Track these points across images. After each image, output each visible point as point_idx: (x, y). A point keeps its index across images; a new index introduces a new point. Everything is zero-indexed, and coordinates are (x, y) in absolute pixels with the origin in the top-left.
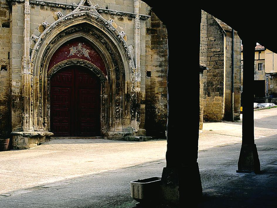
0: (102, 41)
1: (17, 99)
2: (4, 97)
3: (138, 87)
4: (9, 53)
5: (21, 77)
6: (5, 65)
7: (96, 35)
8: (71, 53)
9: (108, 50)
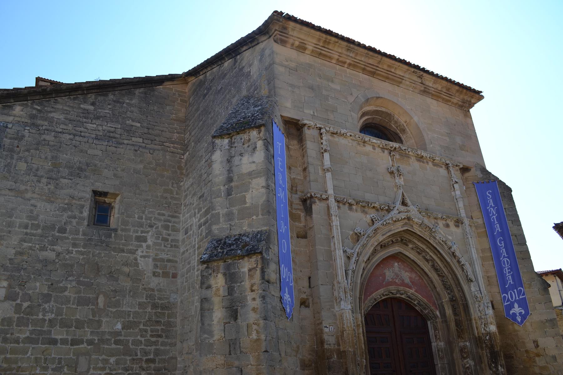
0: (428, 257)
1: (334, 355)
2: (310, 354)
3: (491, 324)
5: (335, 315)
6: (305, 297)
7: (418, 248)
8: (387, 278)
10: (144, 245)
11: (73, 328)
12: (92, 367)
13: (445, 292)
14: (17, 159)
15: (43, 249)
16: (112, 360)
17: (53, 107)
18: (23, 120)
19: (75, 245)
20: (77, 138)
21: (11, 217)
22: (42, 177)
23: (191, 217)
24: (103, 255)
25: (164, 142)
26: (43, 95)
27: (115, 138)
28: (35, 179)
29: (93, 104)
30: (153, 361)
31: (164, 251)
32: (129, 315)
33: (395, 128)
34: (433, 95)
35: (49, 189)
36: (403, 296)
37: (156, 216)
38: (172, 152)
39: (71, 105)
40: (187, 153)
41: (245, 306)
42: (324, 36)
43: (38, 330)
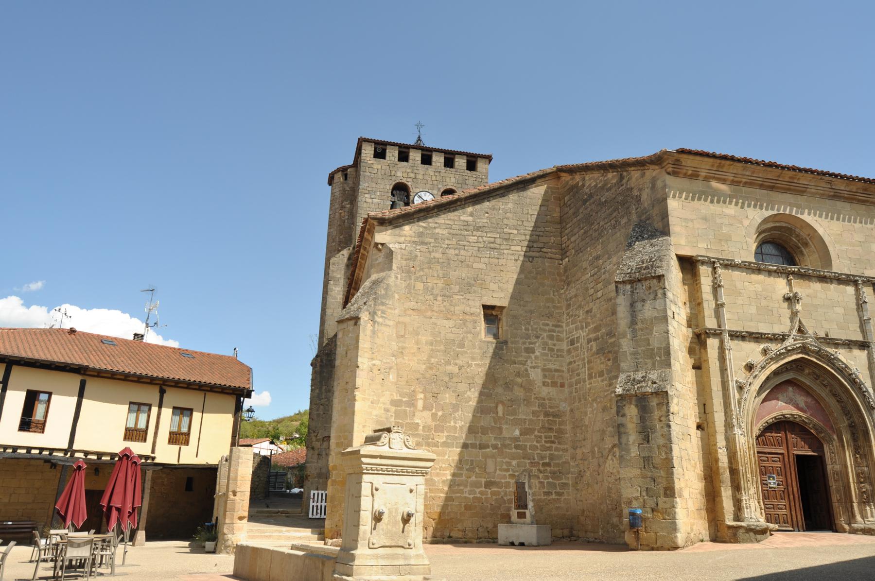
4: (704, 405)
9: (834, 395)
10: (533, 356)
11: (480, 434)
12: (498, 468)
13: (844, 417)
14: (415, 280)
15: (448, 363)
16: (514, 463)
17: (436, 223)
18: (413, 239)
19: (473, 359)
20: (463, 252)
21: (418, 334)
22: (437, 295)
23: (577, 329)
24: (498, 367)
25: (542, 248)
26: (427, 212)
27: (495, 249)
28: (431, 298)
29: (471, 215)
30: (548, 465)
31: (551, 361)
32: (525, 423)
33: (797, 241)
34: (845, 198)
35: (445, 306)
36: (797, 420)
37: (542, 327)
38: (551, 258)
39: (452, 218)
40: (567, 259)
41: (655, 432)
42: (718, 161)
43: (452, 436)
